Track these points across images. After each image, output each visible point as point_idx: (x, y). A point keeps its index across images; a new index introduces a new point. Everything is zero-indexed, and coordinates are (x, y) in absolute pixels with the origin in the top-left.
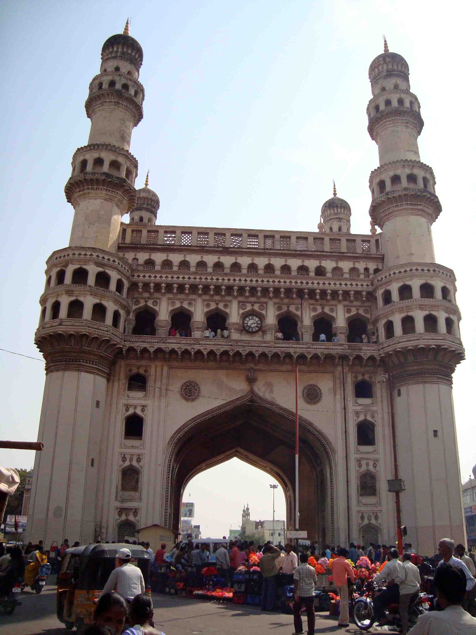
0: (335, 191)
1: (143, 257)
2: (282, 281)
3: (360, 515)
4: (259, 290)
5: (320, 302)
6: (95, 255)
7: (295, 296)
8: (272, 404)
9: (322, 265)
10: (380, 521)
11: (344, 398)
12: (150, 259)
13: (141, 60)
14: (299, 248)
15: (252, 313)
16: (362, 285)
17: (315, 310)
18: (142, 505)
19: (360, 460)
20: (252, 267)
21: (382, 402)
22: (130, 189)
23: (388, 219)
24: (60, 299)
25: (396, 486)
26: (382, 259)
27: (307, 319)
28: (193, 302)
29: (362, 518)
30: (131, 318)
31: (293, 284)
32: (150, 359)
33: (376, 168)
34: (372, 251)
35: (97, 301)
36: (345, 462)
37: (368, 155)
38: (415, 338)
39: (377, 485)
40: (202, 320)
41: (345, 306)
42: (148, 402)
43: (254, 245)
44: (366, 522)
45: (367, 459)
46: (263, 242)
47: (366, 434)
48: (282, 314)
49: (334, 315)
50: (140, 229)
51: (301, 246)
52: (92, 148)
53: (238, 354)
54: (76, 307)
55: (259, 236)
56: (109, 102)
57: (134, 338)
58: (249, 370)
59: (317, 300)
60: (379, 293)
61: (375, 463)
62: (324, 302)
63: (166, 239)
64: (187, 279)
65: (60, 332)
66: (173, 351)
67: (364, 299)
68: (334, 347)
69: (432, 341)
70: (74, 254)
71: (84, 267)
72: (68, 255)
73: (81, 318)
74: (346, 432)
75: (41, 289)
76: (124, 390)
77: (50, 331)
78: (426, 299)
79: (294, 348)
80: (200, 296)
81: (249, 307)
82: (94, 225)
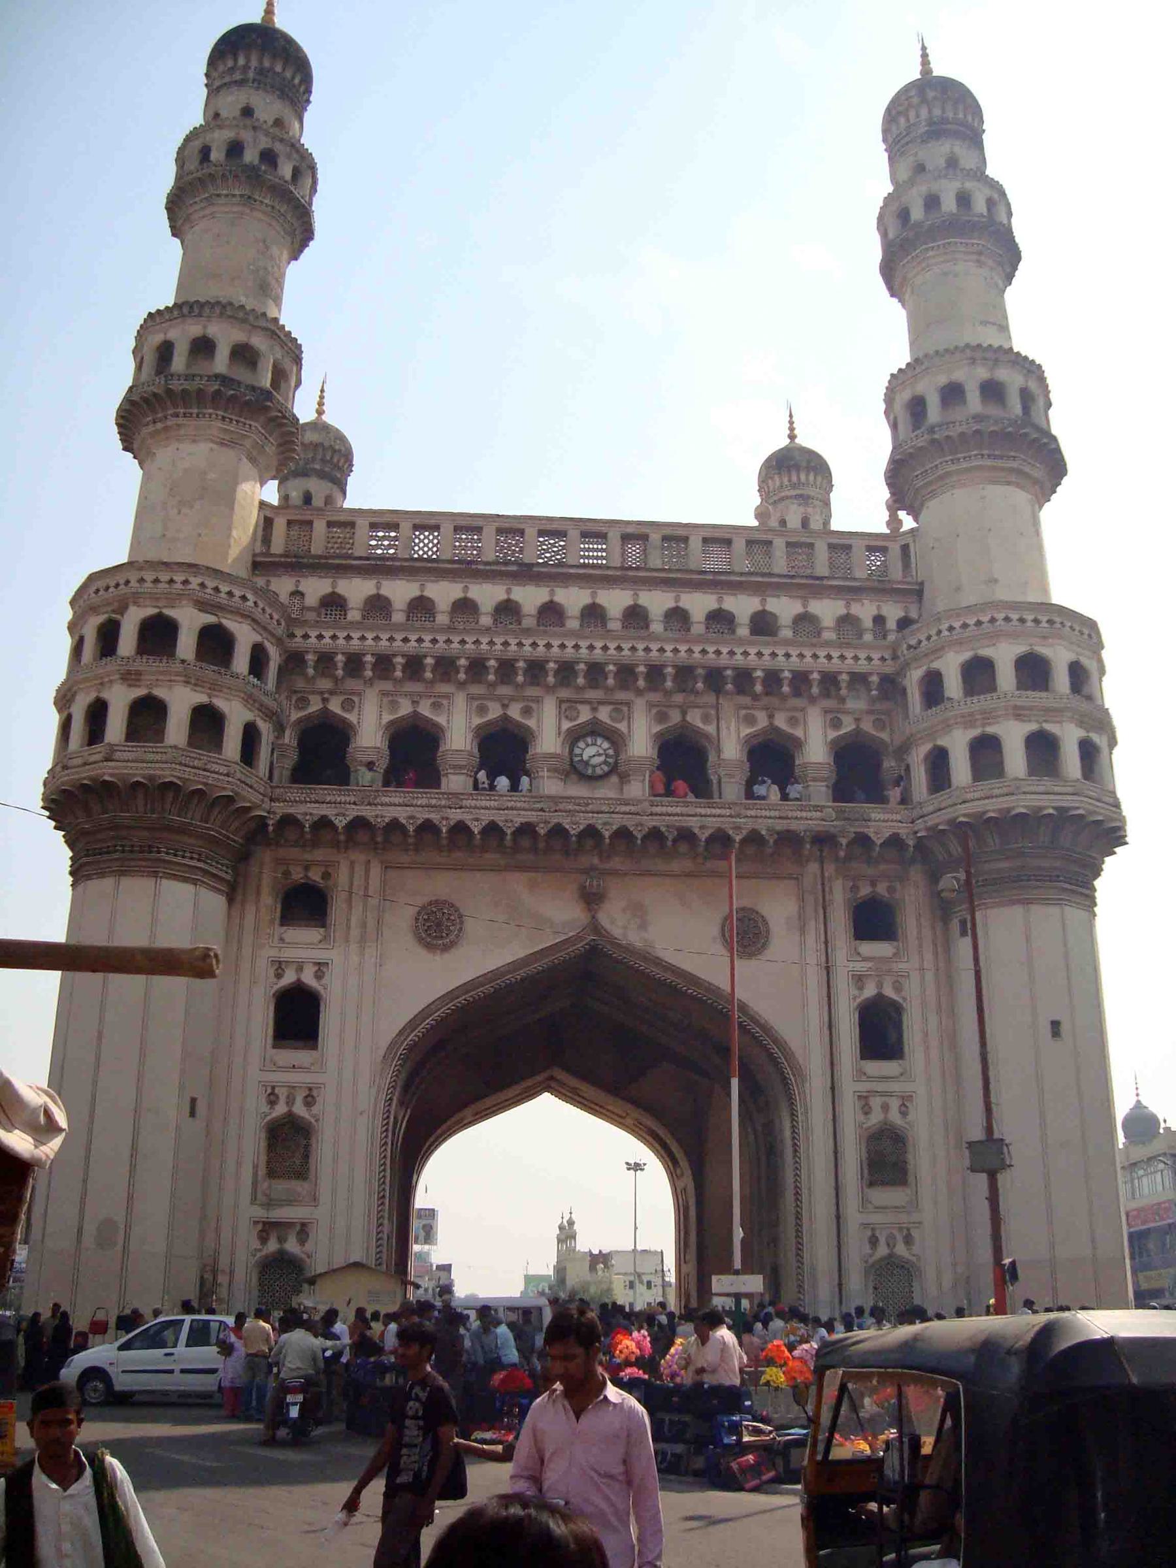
0: (792, 429)
1: (315, 588)
2: (669, 648)
3: (869, 1233)
4: (610, 671)
5: (766, 700)
6: (195, 581)
7: (700, 685)
8: (647, 957)
9: (769, 608)
10: (916, 1249)
11: (826, 943)
12: (334, 593)
13: (309, 91)
14: (708, 566)
15: (594, 730)
16: (869, 659)
17: (750, 720)
18: (319, 1214)
19: (866, 1097)
20: (593, 614)
21: (920, 946)
22: (284, 417)
23: (933, 494)
24: (105, 695)
25: (988, 1156)
26: (918, 593)
27: (730, 744)
28: (445, 702)
30: (287, 741)
31: (697, 655)
32: (336, 845)
33: (904, 367)
34: (891, 572)
35: (201, 698)
36: (830, 1100)
37: (885, 336)
38: (1005, 790)
39: (910, 1157)
40: (468, 748)
41: (826, 712)
42: (332, 955)
43: (597, 558)
44: (882, 1250)
46: (617, 550)
47: (880, 1032)
48: (668, 730)
49: (798, 733)
50: (310, 518)
51: (715, 562)
52: (185, 310)
53: (558, 831)
54: (148, 715)
55: (610, 535)
56: (227, 196)
57: (296, 792)
58: (588, 871)
59: (755, 697)
60: (913, 679)
61: (903, 1104)
62: (775, 701)
63: (373, 543)
64: (427, 643)
65: (107, 778)
66: (395, 826)
67: (874, 692)
68: (799, 814)
69: (1046, 797)
70: (142, 580)
71: (168, 612)
72: (127, 582)
73: (162, 741)
75: (57, 669)
76: (272, 922)
77: (85, 775)
78: (1029, 693)
80: (462, 685)
81: (585, 715)
82: (192, 507)
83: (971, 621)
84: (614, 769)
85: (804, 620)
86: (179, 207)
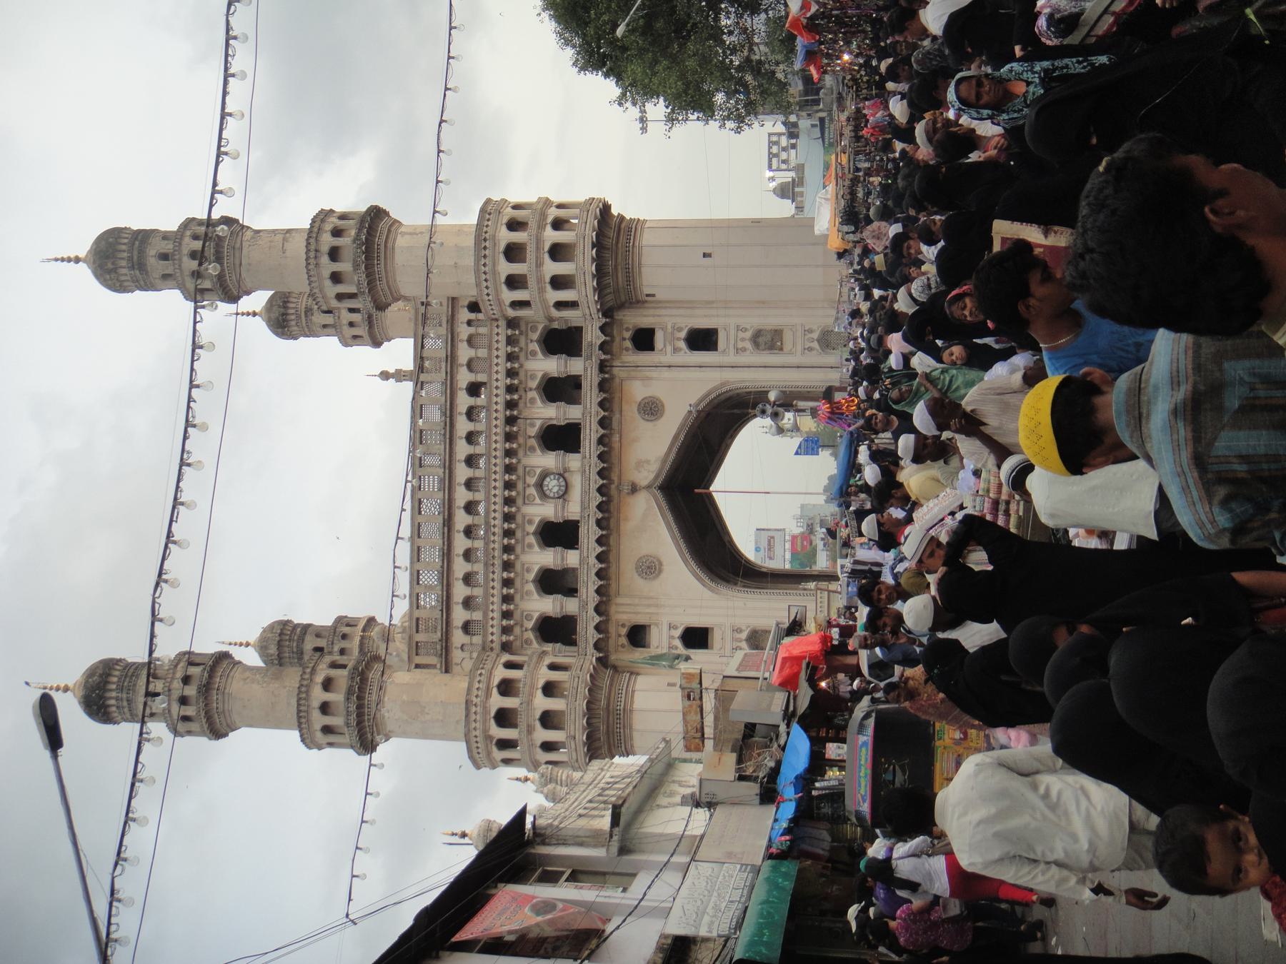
1: (458, 637)
7: (515, 429)
8: (664, 461)
10: (815, 327)
15: (540, 485)
17: (532, 401)
26: (453, 301)
29: (810, 349)
31: (498, 430)
32: (607, 621)
35: (539, 693)
44: (816, 345)
46: (429, 470)
49: (540, 375)
51: (434, 415)
53: (599, 507)
54: (548, 720)
60: (511, 313)
71: (493, 714)
77: (583, 750)
80: (517, 557)
81: (532, 491)
83: (485, 284)
84: (561, 475)
85: (470, 365)
86: (217, 732)
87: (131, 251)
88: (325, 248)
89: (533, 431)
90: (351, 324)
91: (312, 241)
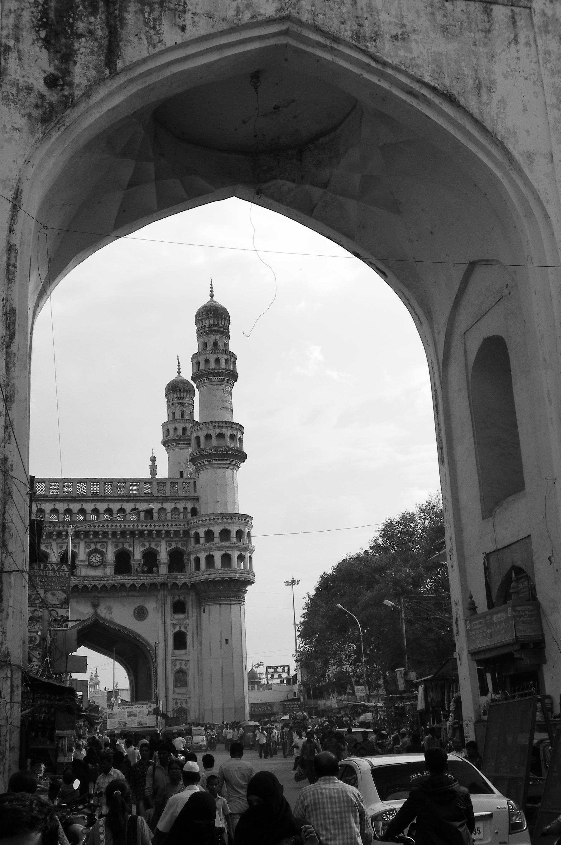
10: (189, 705)
15: (96, 551)
16: (180, 525)
17: (144, 545)
21: (192, 615)
26: (197, 499)
27: (137, 555)
29: (176, 703)
43: (96, 490)
45: (179, 660)
49: (158, 549)
60: (192, 533)
74: (165, 641)
79: (127, 580)
80: (54, 540)
81: (93, 547)
83: (208, 519)
85: (162, 510)
87: (218, 326)
88: (224, 431)
89: (127, 546)
90: (176, 429)
91: (227, 424)
